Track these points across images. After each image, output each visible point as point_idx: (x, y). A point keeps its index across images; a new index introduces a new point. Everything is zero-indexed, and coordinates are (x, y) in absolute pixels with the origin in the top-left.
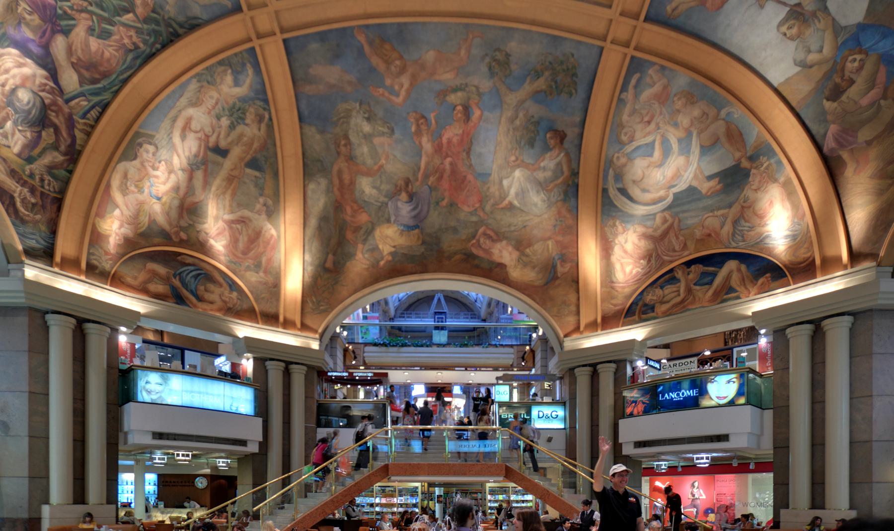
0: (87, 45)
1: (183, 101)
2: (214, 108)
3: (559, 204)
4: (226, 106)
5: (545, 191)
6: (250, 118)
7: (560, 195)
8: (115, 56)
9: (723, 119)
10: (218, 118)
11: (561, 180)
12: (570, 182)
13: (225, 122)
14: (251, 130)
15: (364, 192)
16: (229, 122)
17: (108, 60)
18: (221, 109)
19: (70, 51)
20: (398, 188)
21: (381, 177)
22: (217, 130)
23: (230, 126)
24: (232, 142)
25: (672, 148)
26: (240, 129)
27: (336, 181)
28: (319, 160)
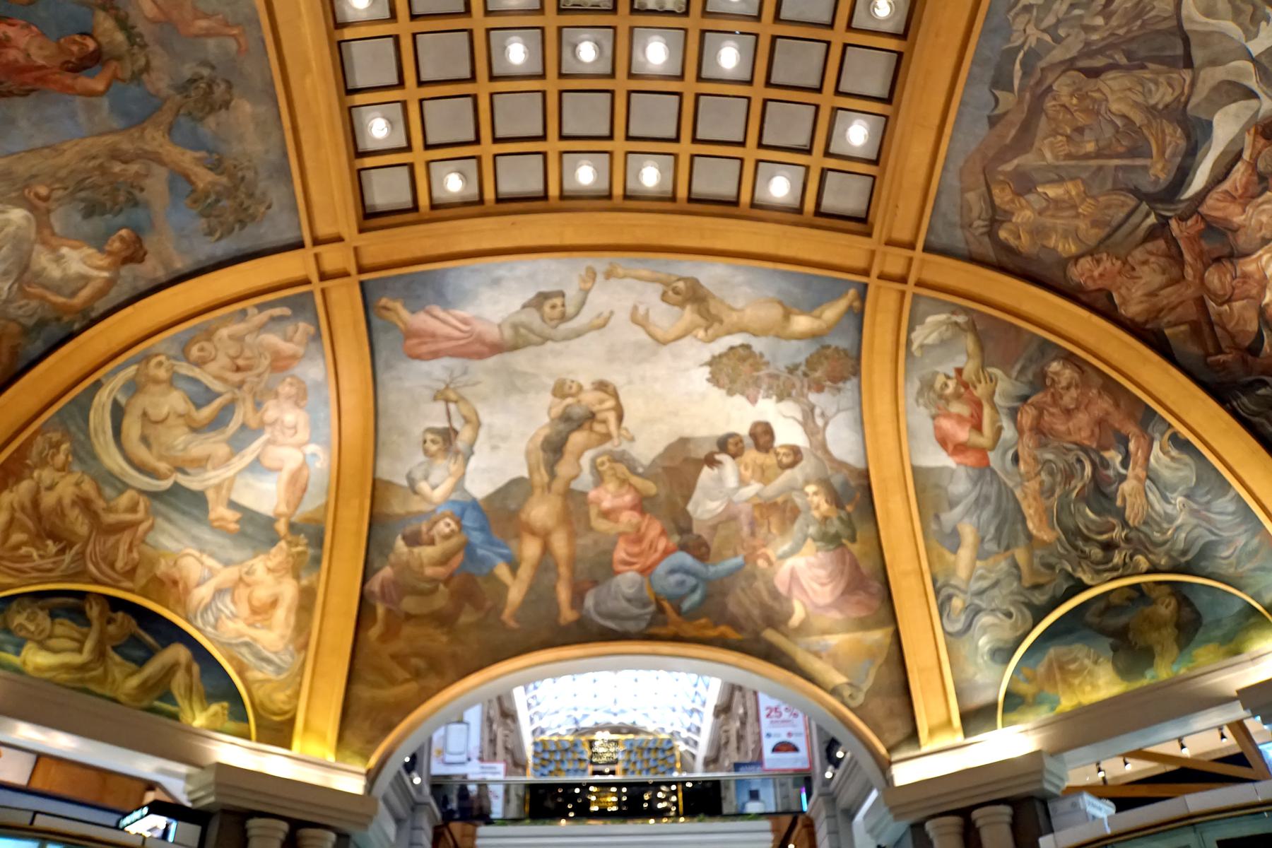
3: (14, 328)
5: (16, 286)
7: (31, 316)
9: (305, 455)
11: (60, 300)
12: (66, 319)
25: (227, 425)
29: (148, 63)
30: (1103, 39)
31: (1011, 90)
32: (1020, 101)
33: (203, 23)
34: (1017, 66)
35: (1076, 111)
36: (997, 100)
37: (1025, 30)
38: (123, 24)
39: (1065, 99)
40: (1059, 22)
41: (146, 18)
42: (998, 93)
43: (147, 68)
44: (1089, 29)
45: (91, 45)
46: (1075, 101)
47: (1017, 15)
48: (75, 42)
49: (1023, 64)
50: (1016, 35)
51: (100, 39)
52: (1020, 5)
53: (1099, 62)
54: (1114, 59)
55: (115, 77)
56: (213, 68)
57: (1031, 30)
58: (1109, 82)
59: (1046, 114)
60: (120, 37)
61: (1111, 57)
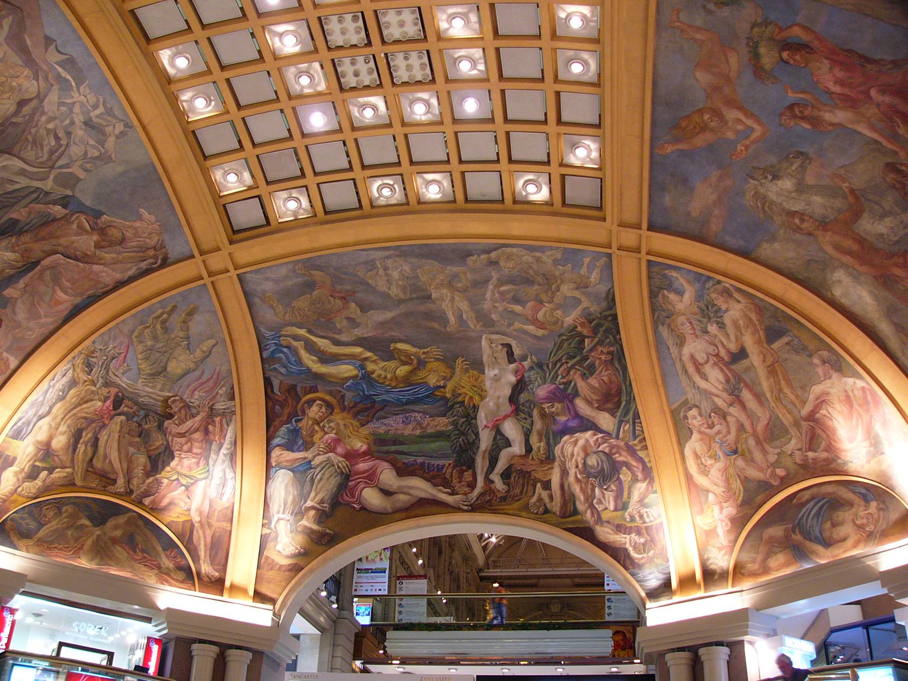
0: (592, 387)
1: (674, 350)
2: (694, 329)
4: (698, 317)
6: (721, 302)
8: (610, 374)
10: (706, 332)
13: (713, 329)
14: (734, 311)
15: (882, 235)
16: (714, 325)
17: (610, 381)
18: (698, 323)
19: (589, 402)
20: (898, 186)
21: (869, 200)
22: (716, 341)
23: (720, 327)
24: (736, 337)
26: (727, 320)
27: (847, 259)
28: (809, 261)
29: (752, 28)
30: (38, 121)
31: (59, 64)
32: (45, 62)
33: (698, 36)
34: (69, 77)
35: (7, 80)
36: (59, 52)
37: (86, 97)
38: (755, 56)
39: (20, 81)
40: (71, 112)
41: (738, 53)
42: (65, 57)
43: (754, 25)
44: (51, 120)
45: (785, 55)
46: (14, 84)
47: (98, 101)
48: (795, 61)
49: (67, 80)
50: (88, 91)
51: (777, 55)
52: (101, 105)
53: (26, 110)
54: (22, 117)
55: (781, 30)
56: (704, 7)
57: (82, 98)
58: (9, 106)
59: (21, 66)
60: (762, 50)
61: (24, 116)
